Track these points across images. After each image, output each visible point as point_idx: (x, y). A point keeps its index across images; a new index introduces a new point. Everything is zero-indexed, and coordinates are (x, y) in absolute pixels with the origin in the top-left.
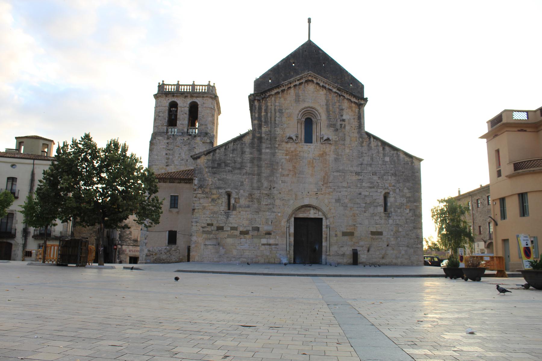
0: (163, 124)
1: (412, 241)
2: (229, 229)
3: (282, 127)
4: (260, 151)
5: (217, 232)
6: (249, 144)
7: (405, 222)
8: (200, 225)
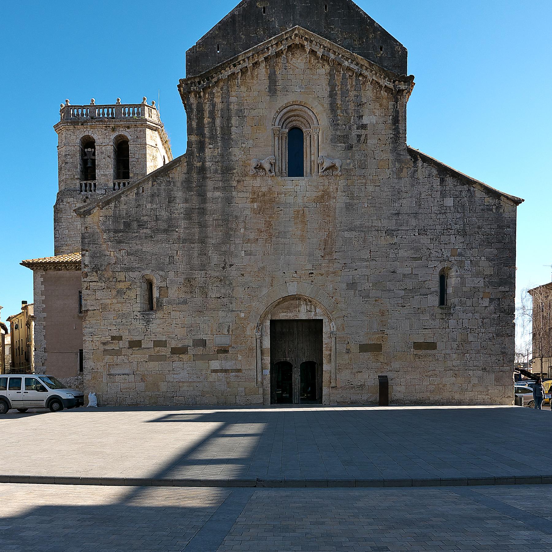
1: (494, 358)
2: (151, 345)
3: (243, 145)
4: (202, 196)
5: (130, 351)
6: (182, 183)
7: (481, 324)
8: (98, 339)
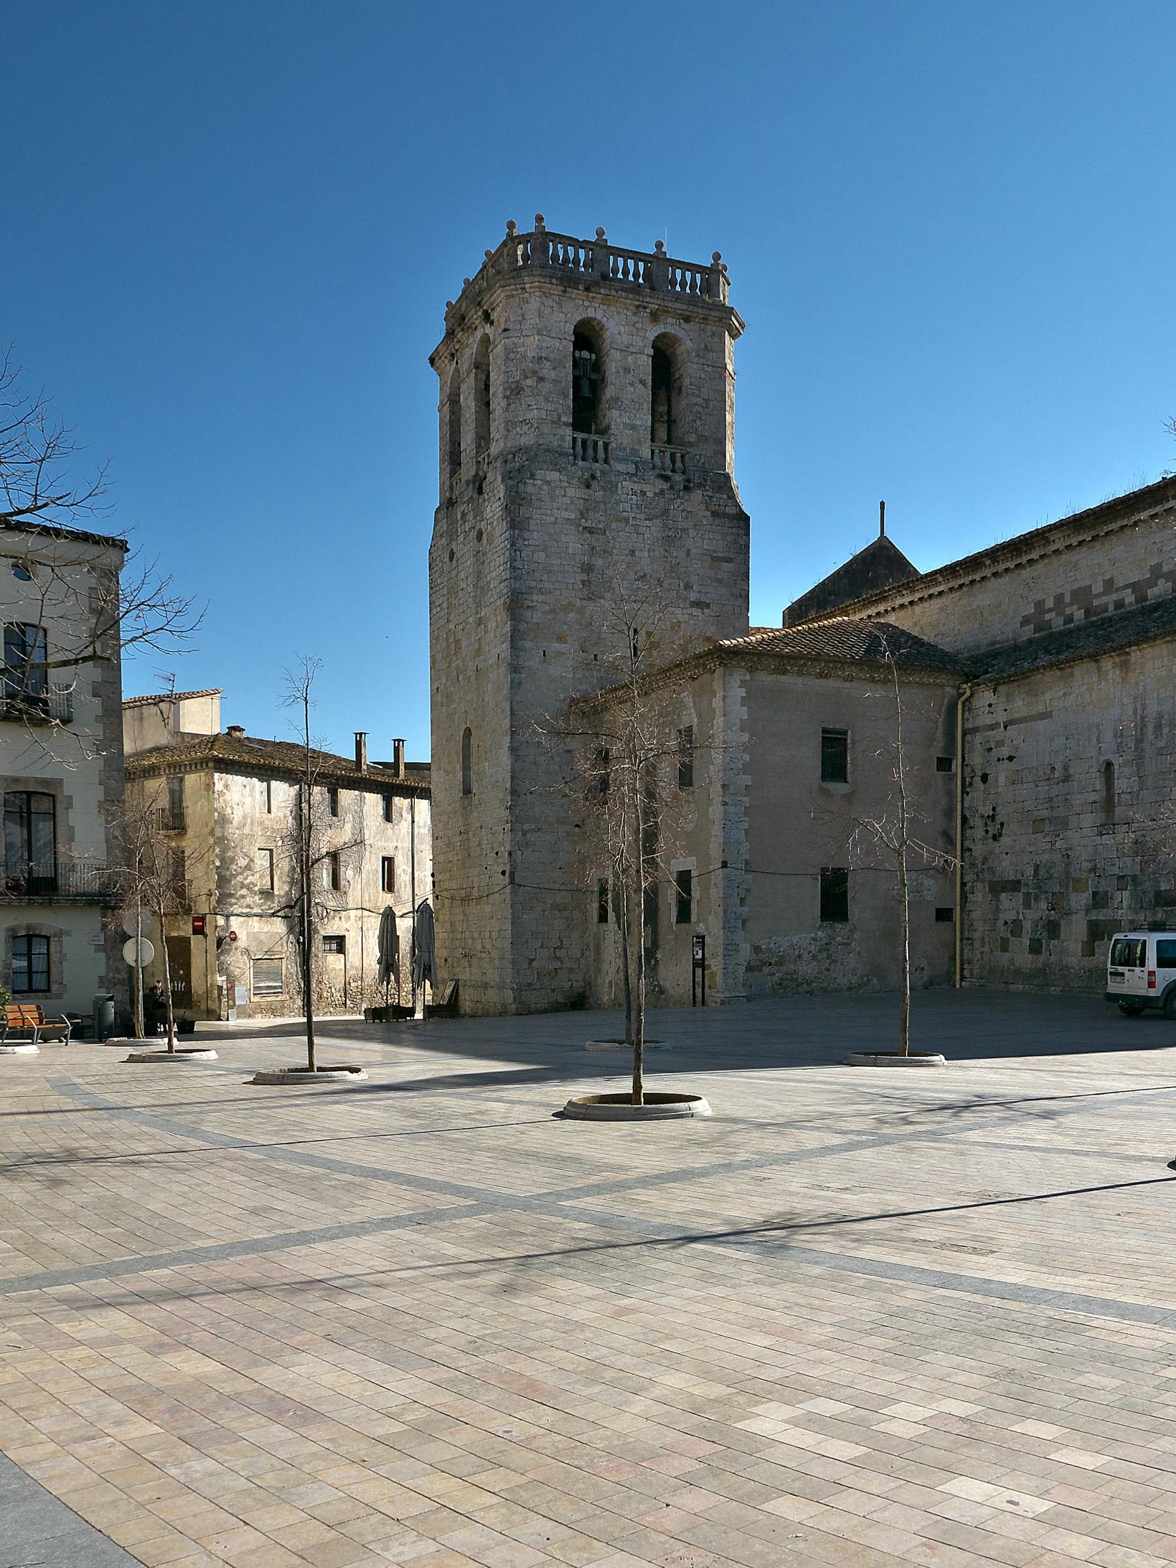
0: (559, 416)
